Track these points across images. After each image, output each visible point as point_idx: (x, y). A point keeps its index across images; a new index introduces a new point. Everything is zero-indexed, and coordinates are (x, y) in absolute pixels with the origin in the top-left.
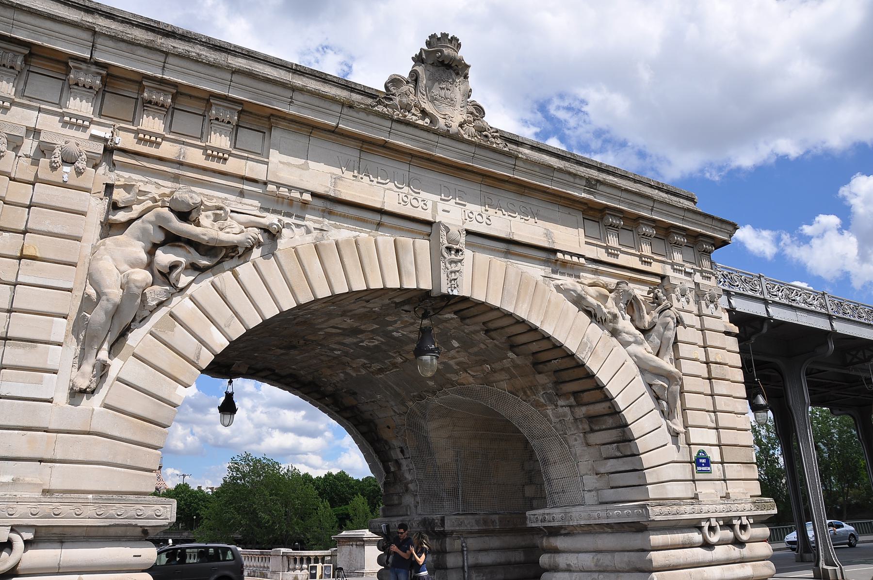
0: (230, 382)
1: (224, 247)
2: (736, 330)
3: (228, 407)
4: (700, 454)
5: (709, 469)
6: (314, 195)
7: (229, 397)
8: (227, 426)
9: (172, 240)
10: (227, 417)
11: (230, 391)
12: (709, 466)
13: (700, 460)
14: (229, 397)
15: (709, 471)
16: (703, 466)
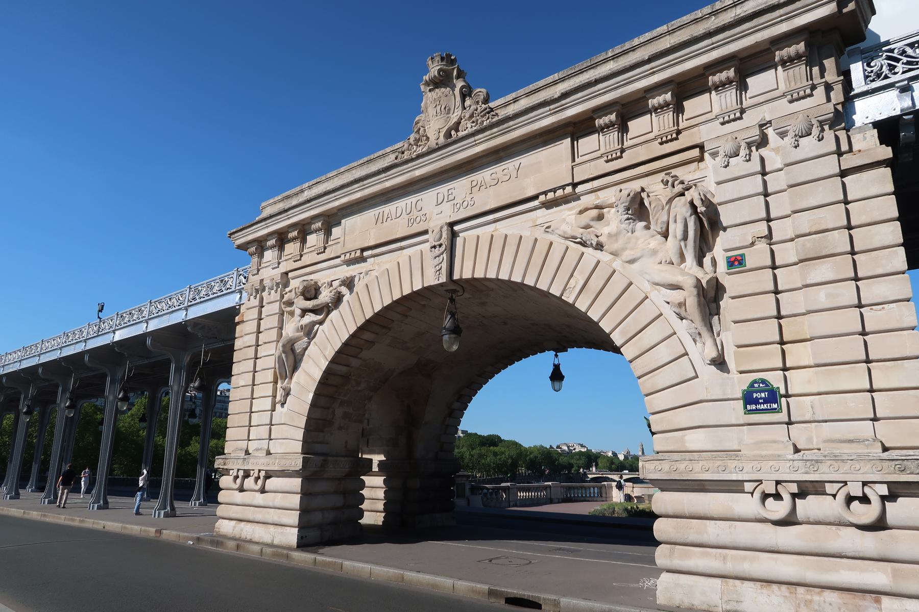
0: (556, 356)
1: (324, 306)
2: (887, 152)
3: (557, 376)
4: (756, 385)
5: (775, 406)
6: (363, 250)
7: (557, 368)
8: (559, 390)
9: (304, 312)
10: (557, 384)
11: (556, 363)
12: (776, 402)
13: (755, 395)
14: (557, 368)
15: (776, 409)
16: (761, 403)
